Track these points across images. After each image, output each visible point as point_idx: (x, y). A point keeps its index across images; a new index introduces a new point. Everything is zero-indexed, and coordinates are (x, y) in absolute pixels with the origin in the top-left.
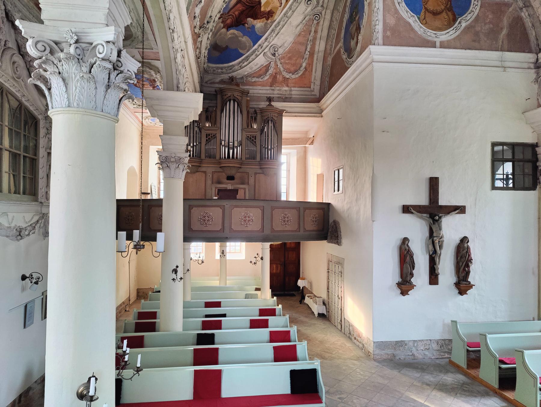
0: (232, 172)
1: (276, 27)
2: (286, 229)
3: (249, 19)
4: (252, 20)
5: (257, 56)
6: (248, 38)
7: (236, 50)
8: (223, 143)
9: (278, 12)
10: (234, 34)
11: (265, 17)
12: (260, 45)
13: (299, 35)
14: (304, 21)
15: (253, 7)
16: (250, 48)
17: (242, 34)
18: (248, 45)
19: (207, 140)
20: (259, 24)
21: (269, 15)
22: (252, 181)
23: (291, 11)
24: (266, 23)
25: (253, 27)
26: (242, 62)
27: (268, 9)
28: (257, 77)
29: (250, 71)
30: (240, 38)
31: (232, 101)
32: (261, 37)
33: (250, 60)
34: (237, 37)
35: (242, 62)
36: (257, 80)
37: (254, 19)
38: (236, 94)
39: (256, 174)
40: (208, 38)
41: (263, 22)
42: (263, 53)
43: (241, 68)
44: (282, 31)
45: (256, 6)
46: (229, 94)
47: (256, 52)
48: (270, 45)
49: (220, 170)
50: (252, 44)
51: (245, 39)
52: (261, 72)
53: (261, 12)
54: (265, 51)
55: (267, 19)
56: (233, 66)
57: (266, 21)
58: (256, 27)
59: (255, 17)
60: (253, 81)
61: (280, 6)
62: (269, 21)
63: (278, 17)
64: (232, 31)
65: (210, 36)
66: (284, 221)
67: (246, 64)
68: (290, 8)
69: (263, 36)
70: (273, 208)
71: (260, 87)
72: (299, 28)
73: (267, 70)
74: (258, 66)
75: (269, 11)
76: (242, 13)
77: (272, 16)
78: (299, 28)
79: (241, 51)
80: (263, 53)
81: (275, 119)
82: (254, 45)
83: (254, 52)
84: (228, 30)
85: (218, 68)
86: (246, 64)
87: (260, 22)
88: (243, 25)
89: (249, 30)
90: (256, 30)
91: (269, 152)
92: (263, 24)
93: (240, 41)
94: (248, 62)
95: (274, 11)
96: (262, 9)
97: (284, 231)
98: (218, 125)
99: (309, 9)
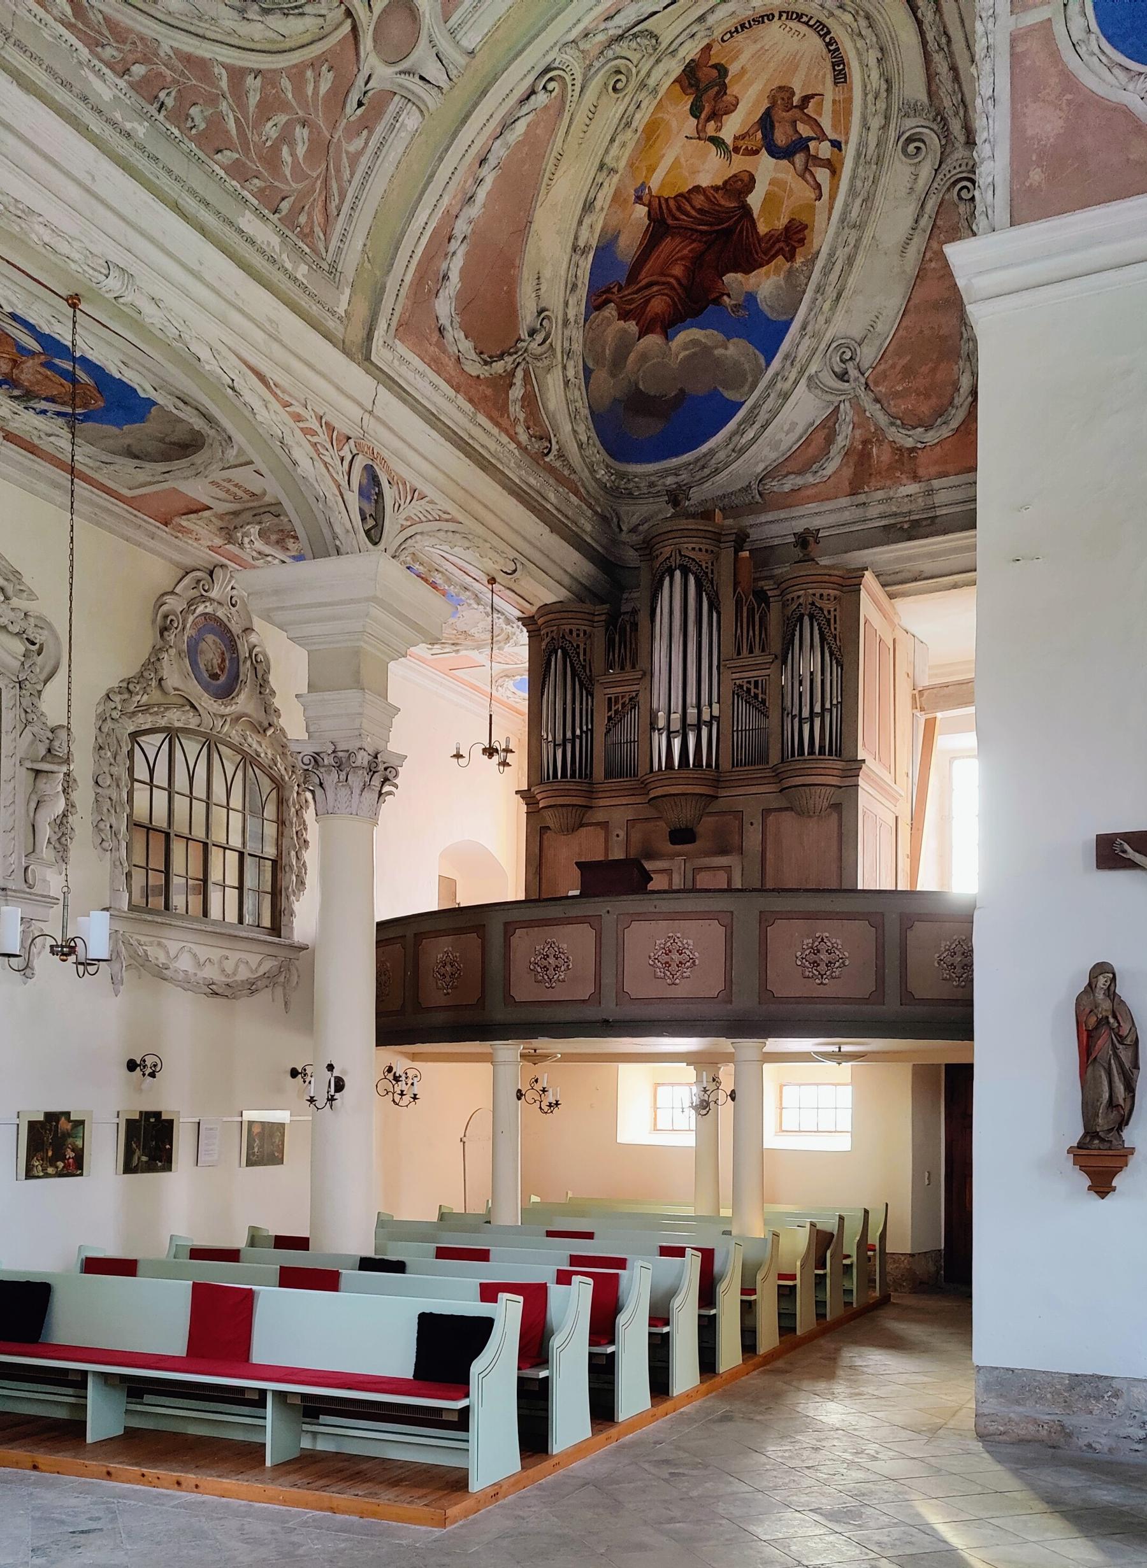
0: (684, 814)
1: (826, 272)
2: (822, 992)
3: (730, 278)
4: (739, 276)
5: (786, 396)
6: (742, 343)
7: (714, 395)
8: (661, 723)
10: (695, 342)
11: (780, 251)
12: (786, 357)
15: (729, 232)
16: (759, 373)
17: (720, 337)
18: (747, 366)
20: (765, 284)
21: (793, 238)
22: (753, 839)
24: (790, 273)
25: (751, 298)
26: (739, 432)
28: (800, 473)
29: (773, 455)
30: (718, 352)
31: (678, 573)
32: (787, 325)
33: (763, 417)
34: (706, 350)
35: (739, 432)
36: (799, 481)
37: (747, 272)
38: (688, 547)
39: (766, 812)
40: (567, 383)
41: (777, 270)
42: (803, 381)
43: (742, 451)
44: (852, 281)
45: (737, 222)
46: (667, 551)
47: (779, 385)
48: (823, 346)
49: (651, 813)
50: (762, 361)
51: (735, 350)
52: (811, 451)
53: (760, 240)
54: (813, 369)
55: (791, 257)
56: (712, 452)
57: (788, 265)
58: (760, 297)
59: (748, 265)
60: (787, 488)
61: (819, 198)
62: (799, 260)
63: (825, 237)
64: (685, 336)
65: (571, 373)
66: (816, 964)
67: (750, 434)
68: (852, 192)
69: (792, 319)
70: (766, 919)
71: (812, 507)
73: (830, 439)
74: (799, 430)
75: (787, 228)
76: (696, 263)
77: (802, 241)
79: (730, 395)
80: (803, 381)
81: (827, 606)
82: (768, 364)
83: (772, 383)
84: (668, 338)
85: (667, 472)
86: (750, 434)
87: (768, 276)
88: (717, 301)
89: (742, 313)
90: (764, 307)
91: (806, 728)
93: (718, 362)
94: (757, 426)
95: (804, 219)
96: (762, 229)
97: (811, 1000)
98: (642, 664)
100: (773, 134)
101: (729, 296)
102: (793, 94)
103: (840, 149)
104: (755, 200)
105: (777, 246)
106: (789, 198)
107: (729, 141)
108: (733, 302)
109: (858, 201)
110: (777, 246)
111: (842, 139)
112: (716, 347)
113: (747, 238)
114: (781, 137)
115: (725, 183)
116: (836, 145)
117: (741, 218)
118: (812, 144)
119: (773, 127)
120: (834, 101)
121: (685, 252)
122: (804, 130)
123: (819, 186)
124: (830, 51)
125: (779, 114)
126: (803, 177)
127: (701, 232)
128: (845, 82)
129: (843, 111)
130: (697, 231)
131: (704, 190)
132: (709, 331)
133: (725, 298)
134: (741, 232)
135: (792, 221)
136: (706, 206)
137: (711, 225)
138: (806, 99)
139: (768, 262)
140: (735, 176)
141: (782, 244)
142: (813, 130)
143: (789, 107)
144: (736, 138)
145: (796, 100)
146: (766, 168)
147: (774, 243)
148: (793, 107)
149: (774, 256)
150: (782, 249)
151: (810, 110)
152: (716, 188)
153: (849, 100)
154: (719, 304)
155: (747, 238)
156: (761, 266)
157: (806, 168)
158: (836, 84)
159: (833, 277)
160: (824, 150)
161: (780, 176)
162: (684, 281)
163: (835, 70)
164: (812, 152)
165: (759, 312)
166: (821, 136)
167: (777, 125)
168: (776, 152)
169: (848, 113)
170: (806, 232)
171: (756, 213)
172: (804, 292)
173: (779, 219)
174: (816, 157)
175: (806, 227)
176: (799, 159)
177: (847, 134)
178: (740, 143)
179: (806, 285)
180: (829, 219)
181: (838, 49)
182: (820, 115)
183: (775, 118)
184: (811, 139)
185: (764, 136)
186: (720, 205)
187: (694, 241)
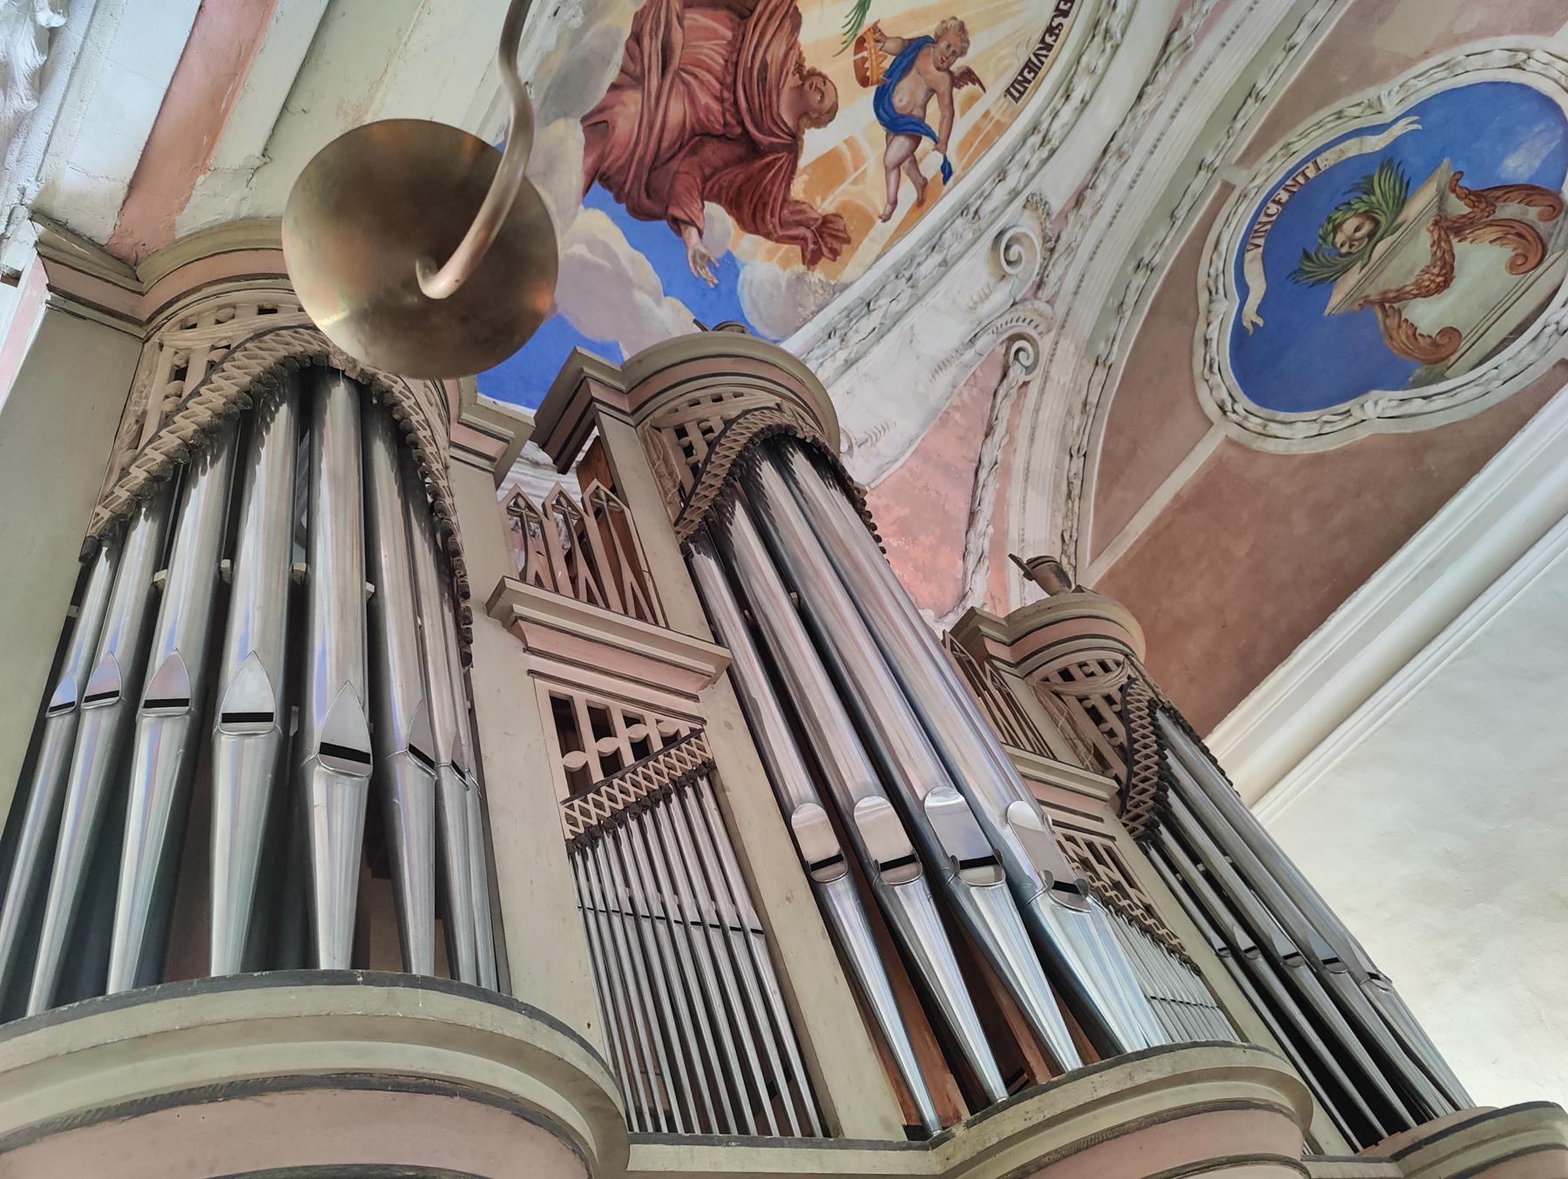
1: (850, 315)
3: (716, 215)
4: (730, 221)
9: (867, 247)
13: (944, 420)
14: (969, 354)
15: (754, 150)
17: (655, 280)
19: (578, 781)
21: (824, 240)
23: (936, 258)
24: (800, 278)
25: (728, 267)
27: (826, 206)
30: (640, 297)
34: (624, 282)
41: (785, 263)
45: (773, 148)
53: (785, 200)
55: (811, 260)
57: (801, 268)
61: (886, 218)
62: (817, 275)
72: (945, 378)
75: (826, 220)
76: (697, 136)
77: (835, 253)
78: (945, 378)
88: (677, 225)
89: (706, 273)
92: (784, 276)
95: (851, 225)
96: (797, 190)
99: (1001, 295)
100: (900, 79)
101: (700, 233)
102: (963, 53)
103: (946, 180)
104: (815, 143)
105: (802, 231)
106: (855, 182)
107: (869, 21)
108: (703, 250)
109: (936, 258)
110: (802, 231)
111: (956, 168)
112: (641, 288)
113: (772, 181)
114: (903, 97)
115: (813, 73)
116: (947, 170)
117: (784, 147)
118: (926, 142)
119: (906, 70)
120: (987, 113)
121: (704, 99)
122: (933, 116)
123: (895, 203)
124: (1043, 41)
125: (927, 63)
126: (888, 171)
127: (736, 103)
128: (1017, 100)
129: (984, 137)
130: (735, 92)
131: (793, 45)
132: (640, 256)
133: (694, 231)
134: (770, 165)
135: (837, 215)
136: (772, 73)
137: (750, 110)
138: (969, 76)
139: (777, 241)
140: (825, 78)
141: (809, 235)
142: (941, 123)
143: (944, 67)
144: (875, 29)
145: (958, 65)
146: (856, 114)
147: (799, 224)
148: (947, 70)
149: (793, 239)
150: (804, 239)
151: (960, 95)
152: (799, 66)
153: (1001, 128)
154: (679, 233)
155: (772, 181)
156: (768, 236)
157: (898, 166)
158: (1008, 91)
159: (866, 325)
160: (930, 164)
161: (863, 143)
162: (665, 144)
163: (1021, 74)
164: (918, 153)
165: (733, 292)
166: (941, 144)
167: (913, 72)
168: (882, 102)
169: (988, 143)
170: (845, 247)
171: (803, 162)
172: (806, 321)
173: (823, 200)
174: (915, 163)
175: (848, 241)
176: (901, 143)
177: (967, 167)
178: (870, 44)
179: (814, 314)
180: (879, 257)
181: (1049, 47)
182: (963, 113)
183: (919, 63)
184: (930, 134)
185: (890, 73)
186: (778, 95)
187: (721, 100)
